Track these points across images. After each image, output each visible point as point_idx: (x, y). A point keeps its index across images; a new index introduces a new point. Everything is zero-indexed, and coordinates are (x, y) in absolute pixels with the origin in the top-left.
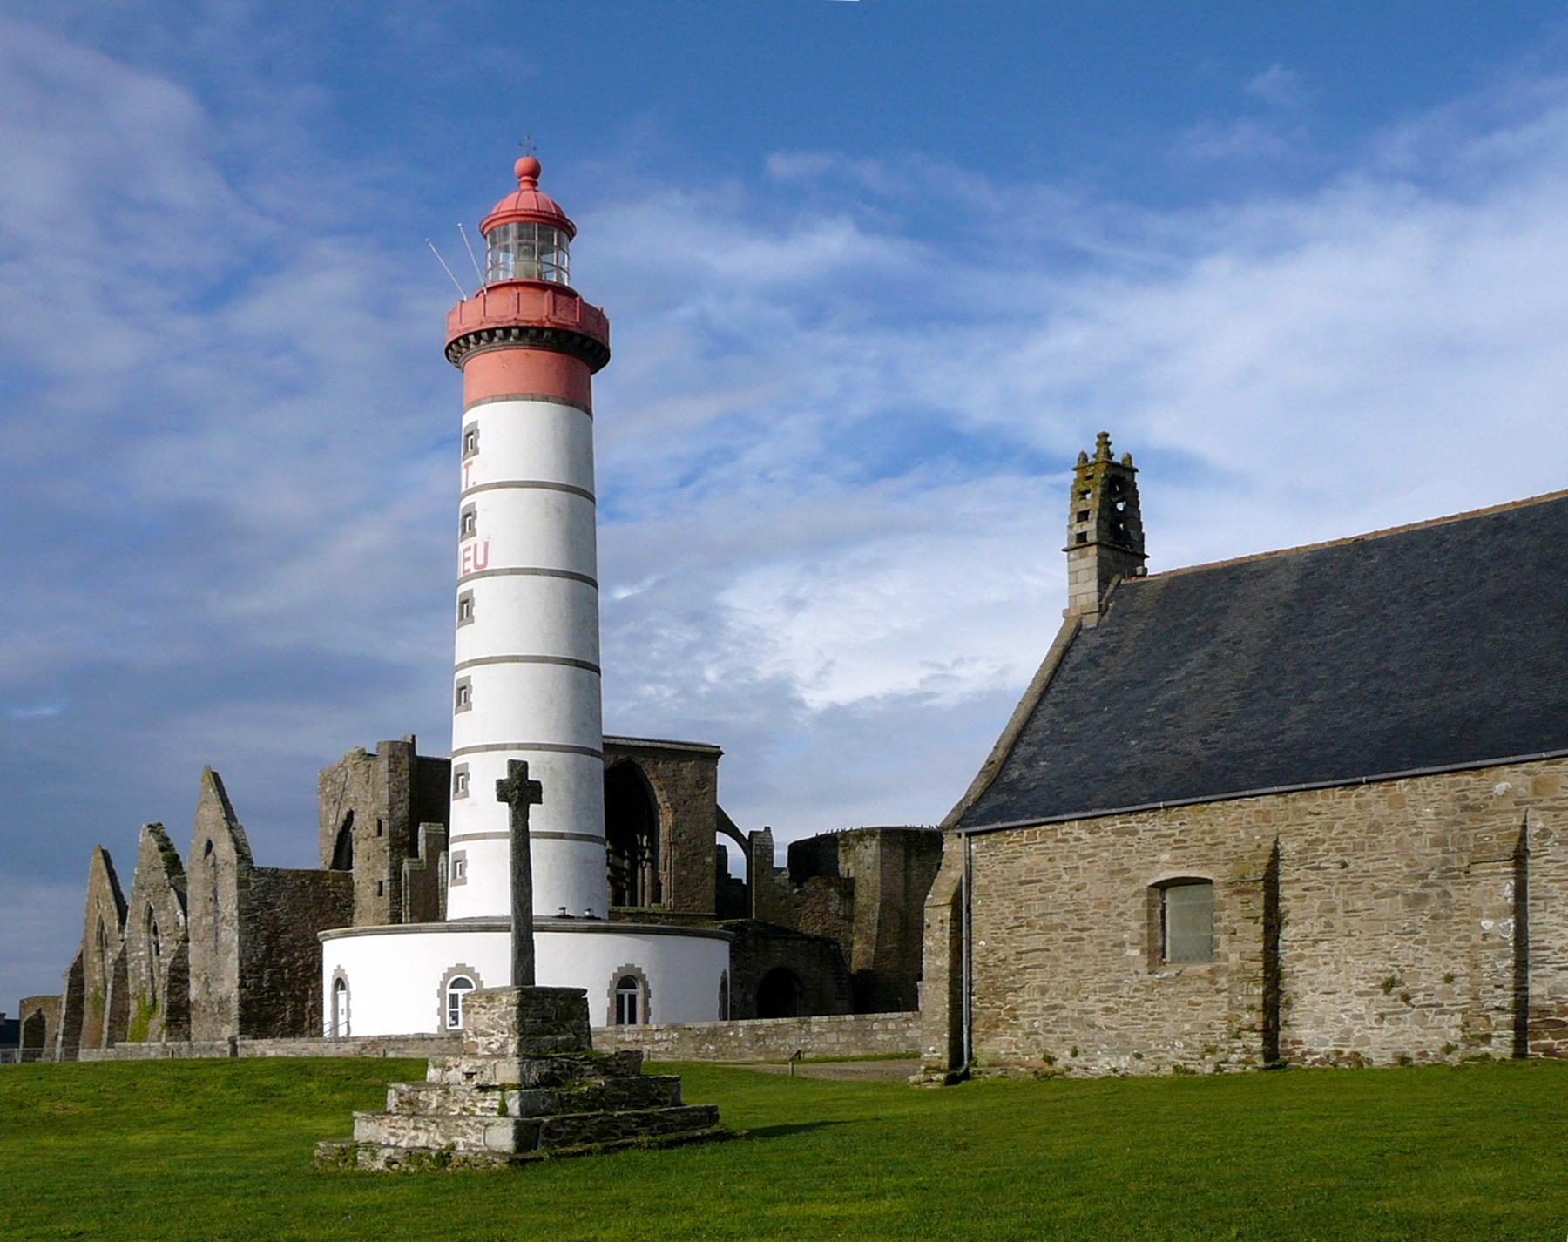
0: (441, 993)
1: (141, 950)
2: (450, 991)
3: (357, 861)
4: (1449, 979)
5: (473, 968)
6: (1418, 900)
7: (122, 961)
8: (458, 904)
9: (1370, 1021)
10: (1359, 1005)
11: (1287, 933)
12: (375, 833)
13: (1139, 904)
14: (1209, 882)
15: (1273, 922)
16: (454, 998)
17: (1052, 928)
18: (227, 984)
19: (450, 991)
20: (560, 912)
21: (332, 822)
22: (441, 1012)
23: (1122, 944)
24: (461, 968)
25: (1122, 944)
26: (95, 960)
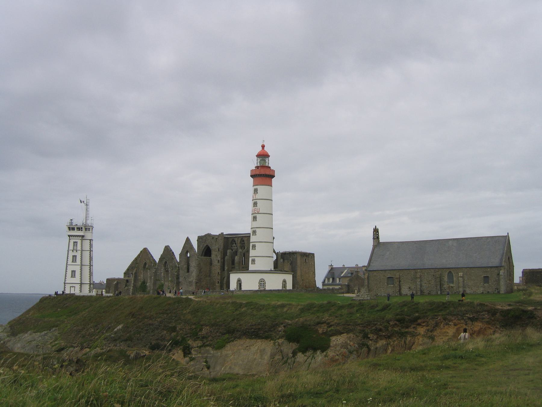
0: (259, 283)
1: (162, 270)
2: (260, 282)
3: (213, 256)
4: (415, 288)
5: (264, 279)
6: (412, 280)
7: (156, 273)
8: (251, 267)
9: (408, 291)
10: (407, 290)
11: (401, 282)
12: (217, 250)
13: (386, 279)
14: (393, 277)
15: (400, 282)
16: (261, 284)
17: (377, 281)
18: (192, 279)
19: (260, 282)
20: (270, 270)
21: (201, 246)
22: (259, 286)
23: (385, 283)
24: (262, 279)
25: (385, 283)
26: (142, 271)
